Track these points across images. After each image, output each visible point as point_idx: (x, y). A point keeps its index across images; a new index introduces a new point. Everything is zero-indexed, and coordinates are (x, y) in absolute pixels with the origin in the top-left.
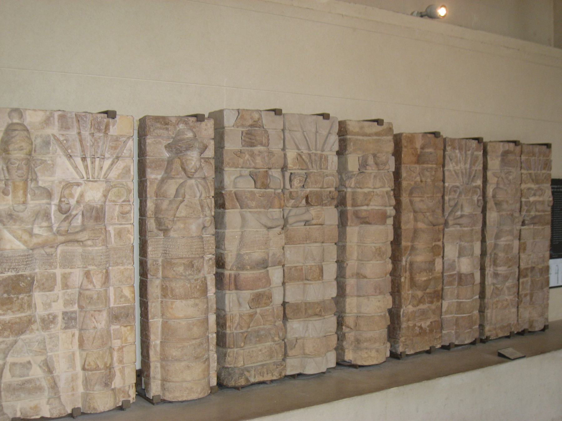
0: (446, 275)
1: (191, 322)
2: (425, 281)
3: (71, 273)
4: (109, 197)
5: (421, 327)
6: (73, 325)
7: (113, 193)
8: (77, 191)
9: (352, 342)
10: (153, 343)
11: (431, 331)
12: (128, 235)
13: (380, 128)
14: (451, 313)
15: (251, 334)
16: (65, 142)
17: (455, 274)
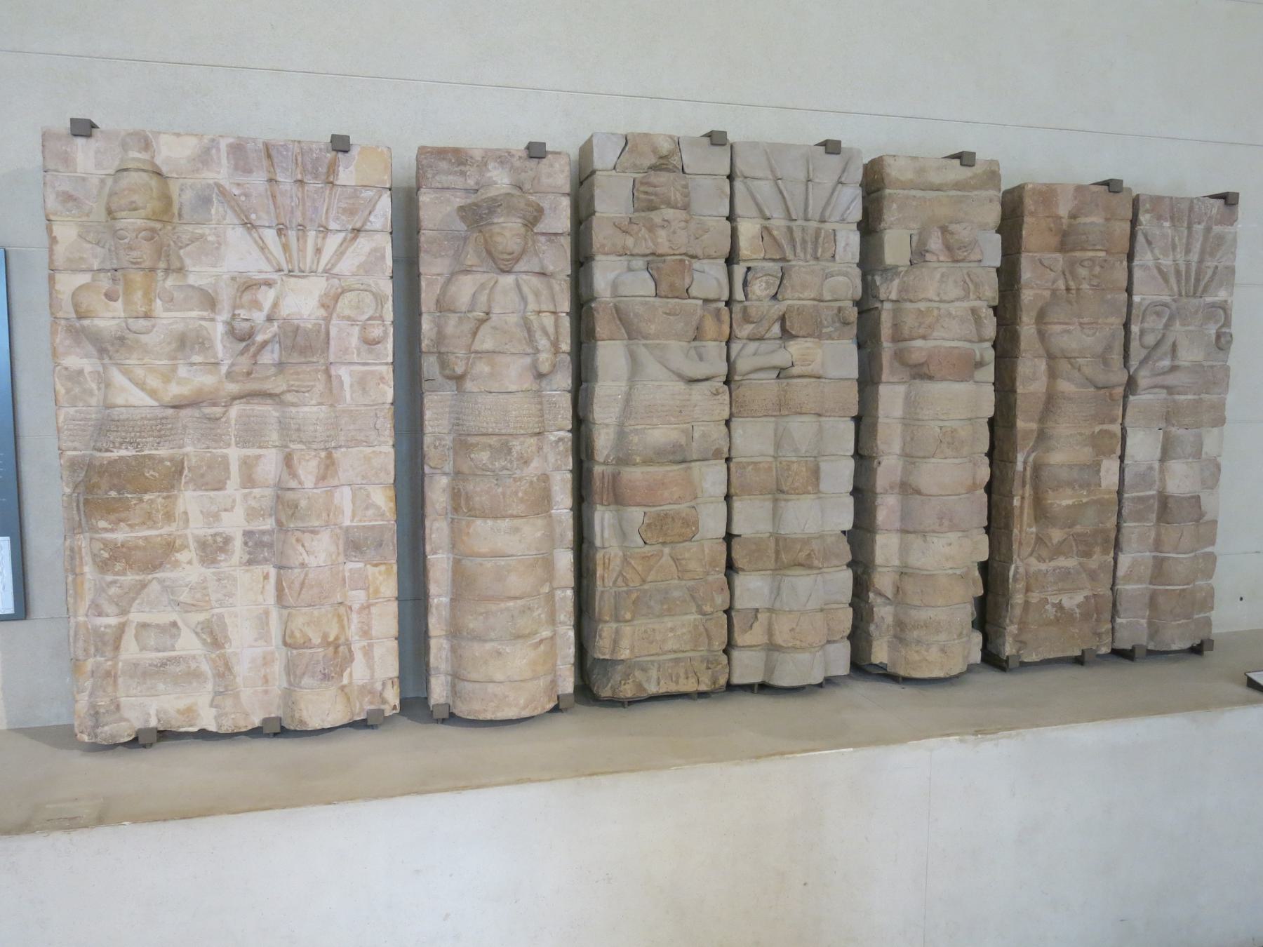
0: (1128, 498)
1: (503, 563)
2: (1068, 507)
3: (260, 456)
4: (338, 309)
5: (1059, 606)
6: (264, 558)
7: (347, 303)
8: (267, 297)
9: (888, 626)
10: (436, 600)
11: (1086, 616)
12: (381, 385)
13: (965, 173)
14: (1139, 581)
15: (650, 596)
16: (243, 198)
17: (1152, 496)
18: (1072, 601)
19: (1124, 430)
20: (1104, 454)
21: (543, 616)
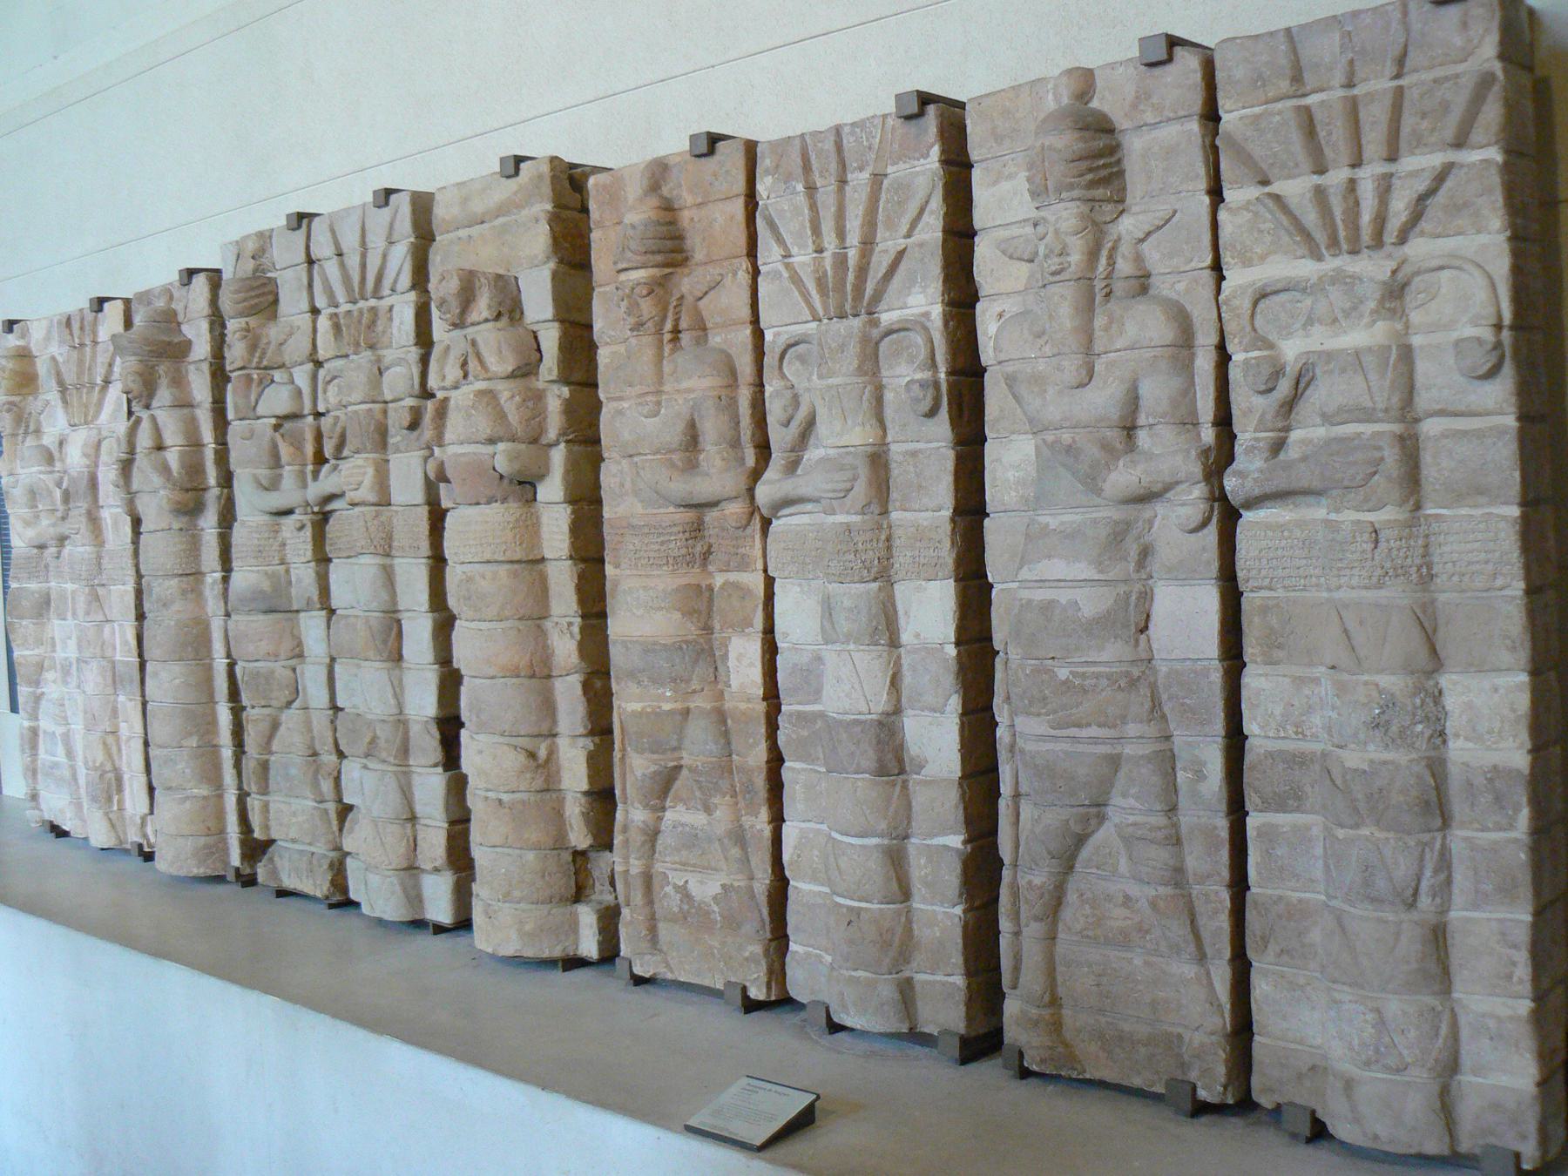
18: (706, 888)
19: (770, 582)
20: (732, 626)
21: (187, 771)
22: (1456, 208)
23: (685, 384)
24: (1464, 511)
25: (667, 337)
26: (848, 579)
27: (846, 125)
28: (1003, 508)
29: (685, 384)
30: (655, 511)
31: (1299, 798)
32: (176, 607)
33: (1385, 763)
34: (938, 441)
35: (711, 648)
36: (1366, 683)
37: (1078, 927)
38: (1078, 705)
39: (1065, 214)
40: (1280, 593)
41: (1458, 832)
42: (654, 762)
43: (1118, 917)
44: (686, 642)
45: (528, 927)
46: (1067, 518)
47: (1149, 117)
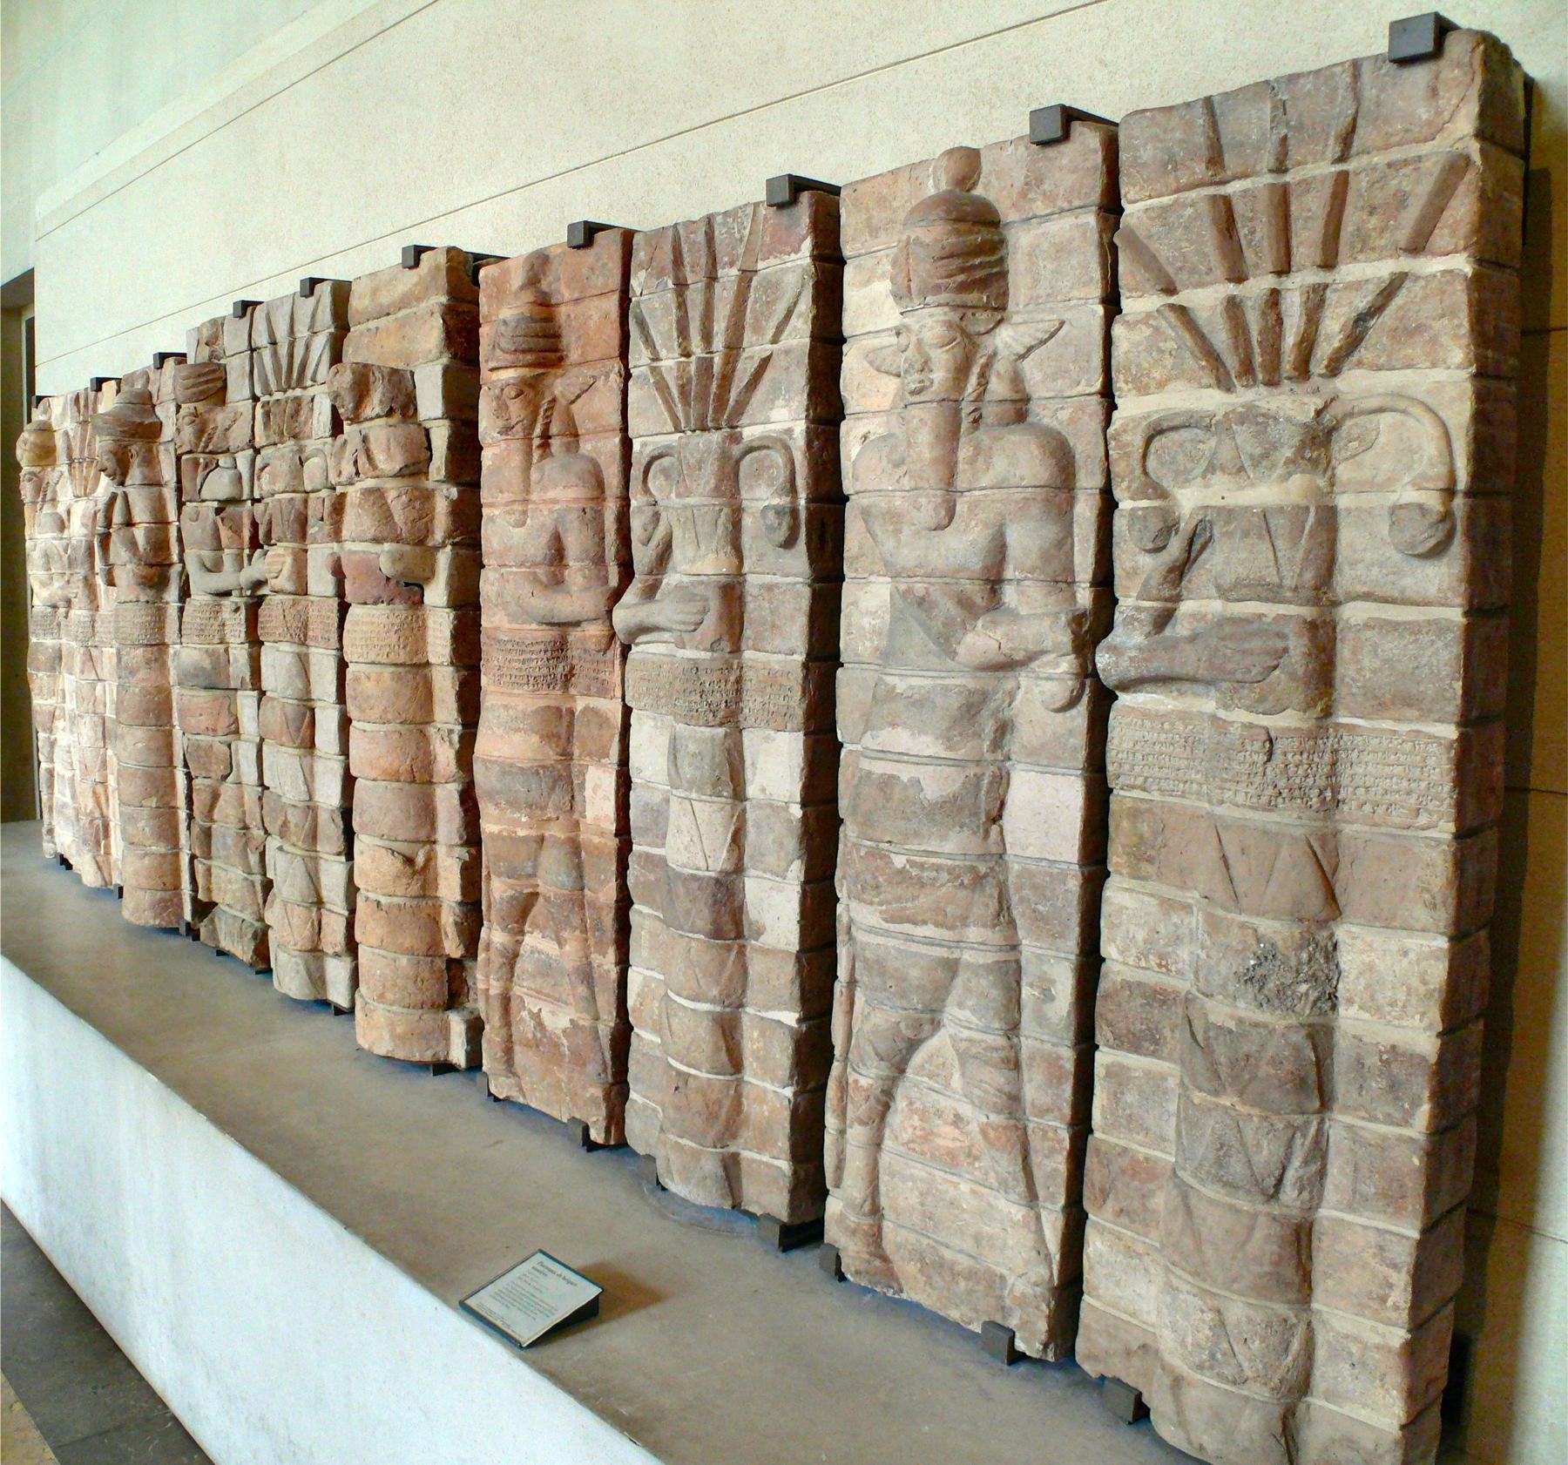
18: (558, 1020)
19: (627, 711)
20: (590, 755)
21: (147, 829)
22: (1408, 332)
23: (551, 494)
24: (1387, 725)
25: (536, 442)
26: (694, 722)
27: (719, 214)
28: (856, 659)
29: (551, 494)
30: (518, 626)
31: (1156, 1042)
32: (141, 674)
33: (1256, 1025)
34: (795, 575)
35: (570, 776)
36: (1243, 926)
37: (905, 1137)
38: (914, 898)
39: (930, 322)
40: (1156, 796)
41: (1340, 1117)
42: (511, 887)
43: (947, 1137)
44: (543, 767)
45: (399, 1030)
46: (916, 682)
47: (1040, 207)
